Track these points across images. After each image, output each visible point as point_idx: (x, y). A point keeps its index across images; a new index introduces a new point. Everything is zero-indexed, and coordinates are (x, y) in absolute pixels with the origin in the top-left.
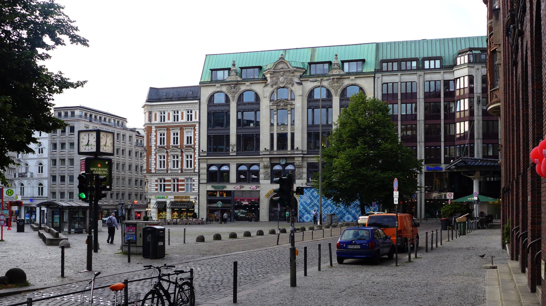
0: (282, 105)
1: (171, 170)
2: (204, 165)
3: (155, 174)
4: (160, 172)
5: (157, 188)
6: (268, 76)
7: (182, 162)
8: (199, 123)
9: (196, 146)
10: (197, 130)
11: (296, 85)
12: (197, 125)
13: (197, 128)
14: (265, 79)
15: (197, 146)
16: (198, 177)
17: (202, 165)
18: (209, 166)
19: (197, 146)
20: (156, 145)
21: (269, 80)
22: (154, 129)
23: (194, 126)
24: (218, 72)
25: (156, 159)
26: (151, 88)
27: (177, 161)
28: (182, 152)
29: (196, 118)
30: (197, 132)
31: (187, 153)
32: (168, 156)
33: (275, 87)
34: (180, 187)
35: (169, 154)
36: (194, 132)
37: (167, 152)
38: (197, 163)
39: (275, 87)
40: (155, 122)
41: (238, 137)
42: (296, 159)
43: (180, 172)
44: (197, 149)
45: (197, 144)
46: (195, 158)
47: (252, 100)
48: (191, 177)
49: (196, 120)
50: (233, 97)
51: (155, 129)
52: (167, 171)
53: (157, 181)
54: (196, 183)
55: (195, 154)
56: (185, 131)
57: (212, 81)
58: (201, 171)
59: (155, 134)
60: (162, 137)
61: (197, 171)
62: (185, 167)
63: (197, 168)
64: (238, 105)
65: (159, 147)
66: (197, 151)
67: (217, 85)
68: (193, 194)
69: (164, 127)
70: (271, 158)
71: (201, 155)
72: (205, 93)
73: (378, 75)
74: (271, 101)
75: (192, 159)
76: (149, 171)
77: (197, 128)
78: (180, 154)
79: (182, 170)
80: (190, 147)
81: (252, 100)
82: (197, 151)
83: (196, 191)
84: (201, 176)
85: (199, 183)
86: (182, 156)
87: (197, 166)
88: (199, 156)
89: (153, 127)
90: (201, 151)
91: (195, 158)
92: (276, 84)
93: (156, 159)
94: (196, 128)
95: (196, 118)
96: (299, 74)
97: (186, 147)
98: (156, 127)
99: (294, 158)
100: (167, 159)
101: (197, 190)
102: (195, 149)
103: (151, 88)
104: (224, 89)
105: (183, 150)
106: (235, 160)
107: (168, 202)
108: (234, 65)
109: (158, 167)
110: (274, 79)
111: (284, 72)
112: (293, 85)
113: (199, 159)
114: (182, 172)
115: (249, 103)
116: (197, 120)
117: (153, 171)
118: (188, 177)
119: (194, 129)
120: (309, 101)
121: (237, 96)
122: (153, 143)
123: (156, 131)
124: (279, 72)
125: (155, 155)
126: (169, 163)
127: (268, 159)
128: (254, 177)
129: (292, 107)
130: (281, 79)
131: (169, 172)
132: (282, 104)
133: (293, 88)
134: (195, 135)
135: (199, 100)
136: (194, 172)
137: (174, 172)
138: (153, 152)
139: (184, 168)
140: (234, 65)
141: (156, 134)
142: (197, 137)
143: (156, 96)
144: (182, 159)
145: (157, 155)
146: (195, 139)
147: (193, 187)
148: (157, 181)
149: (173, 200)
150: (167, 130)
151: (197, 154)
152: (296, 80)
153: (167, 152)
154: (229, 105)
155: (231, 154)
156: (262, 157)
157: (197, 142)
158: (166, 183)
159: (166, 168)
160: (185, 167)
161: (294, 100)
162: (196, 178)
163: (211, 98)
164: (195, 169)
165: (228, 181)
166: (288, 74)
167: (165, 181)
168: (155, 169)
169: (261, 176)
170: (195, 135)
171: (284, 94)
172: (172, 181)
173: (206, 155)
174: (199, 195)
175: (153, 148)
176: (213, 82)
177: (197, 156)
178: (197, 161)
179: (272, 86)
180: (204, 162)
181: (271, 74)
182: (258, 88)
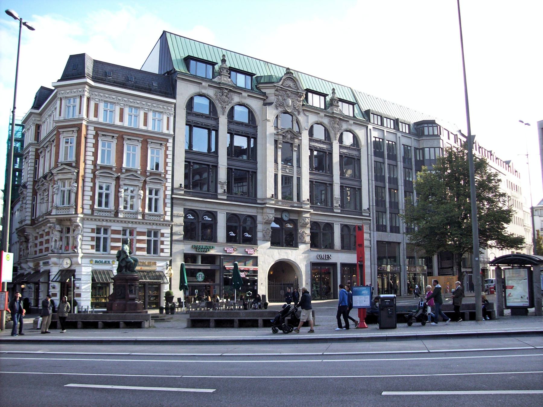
10: (170, 149)
12: (171, 141)
13: (170, 145)
15: (169, 176)
20: (94, 163)
23: (167, 141)
24: (198, 63)
30: (169, 153)
32: (118, 186)
33: (280, 109)
35: (121, 183)
41: (229, 170)
43: (140, 217)
45: (170, 172)
47: (245, 119)
51: (94, 133)
53: (93, 231)
60: (69, 145)
63: (169, 213)
65: (102, 167)
66: (169, 185)
67: (204, 84)
68: (163, 259)
72: (185, 91)
77: (170, 145)
81: (245, 119)
85: (171, 241)
86: (144, 189)
87: (168, 209)
88: (173, 193)
90: (176, 185)
95: (168, 129)
101: (169, 251)
106: (225, 207)
108: (224, 61)
113: (172, 199)
123: (96, 137)
128: (247, 235)
131: (121, 215)
132: (289, 136)
140: (224, 61)
141: (97, 141)
142: (169, 160)
146: (166, 164)
151: (169, 188)
154: (217, 119)
157: (169, 168)
165: (213, 238)
169: (259, 235)
170: (166, 156)
177: (169, 193)
179: (277, 108)
181: (277, 90)
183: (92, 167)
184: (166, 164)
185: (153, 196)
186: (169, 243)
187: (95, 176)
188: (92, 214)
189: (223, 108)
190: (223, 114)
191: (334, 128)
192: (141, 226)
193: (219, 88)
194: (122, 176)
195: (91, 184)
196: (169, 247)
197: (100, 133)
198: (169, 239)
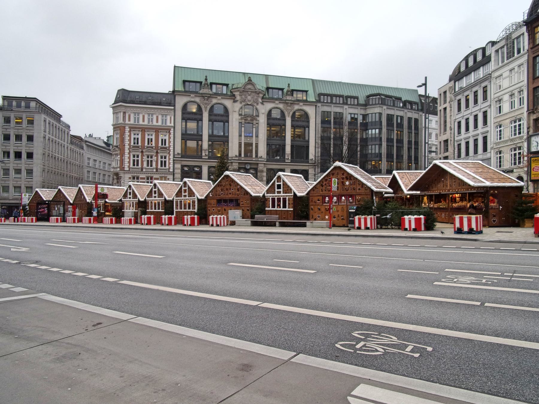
0: (249, 120)
1: (146, 169)
2: (178, 166)
3: (129, 172)
4: (134, 170)
6: (237, 94)
7: (157, 162)
8: (174, 128)
11: (260, 104)
12: (172, 129)
13: (172, 132)
14: (234, 95)
15: (172, 148)
17: (176, 166)
18: (183, 166)
19: (172, 148)
20: (129, 145)
21: (238, 98)
22: (127, 129)
23: (170, 130)
26: (123, 90)
27: (151, 161)
28: (157, 153)
29: (171, 123)
30: (172, 136)
31: (161, 154)
32: (142, 156)
33: (243, 104)
35: (144, 154)
36: (169, 135)
37: (142, 152)
38: (172, 164)
39: (243, 104)
40: (129, 123)
42: (259, 165)
43: (155, 170)
44: (172, 151)
45: (172, 146)
46: (169, 159)
48: (166, 175)
49: (170, 125)
50: (206, 108)
51: (129, 130)
52: (142, 169)
53: (130, 178)
55: (170, 155)
56: (160, 134)
58: (176, 171)
59: (129, 134)
61: (171, 170)
62: (159, 167)
63: (172, 168)
64: (210, 115)
65: (133, 147)
66: (172, 153)
67: (192, 95)
69: (139, 128)
70: (239, 163)
72: (180, 101)
73: (319, 105)
74: (240, 115)
76: (122, 169)
78: (155, 154)
79: (157, 169)
80: (166, 148)
82: (172, 153)
86: (157, 156)
87: (171, 166)
88: (174, 157)
90: (176, 153)
91: (169, 159)
92: (244, 101)
95: (171, 123)
96: (261, 95)
97: (161, 148)
98: (130, 128)
99: (258, 164)
100: (142, 158)
102: (170, 150)
104: (198, 100)
106: (207, 163)
108: (206, 80)
109: (131, 166)
110: (243, 96)
111: (251, 92)
112: (258, 104)
113: (174, 160)
114: (157, 171)
115: (219, 115)
116: (172, 125)
118: (163, 175)
119: (169, 132)
120: (268, 119)
121: (209, 107)
122: (127, 143)
123: (130, 131)
124: (248, 92)
125: (129, 153)
127: (237, 164)
129: (257, 122)
130: (249, 98)
131: (144, 170)
132: (249, 119)
133: (258, 107)
134: (170, 138)
135: (174, 106)
136: (169, 172)
137: (148, 170)
138: (127, 151)
140: (206, 80)
142: (172, 140)
143: (126, 98)
144: (157, 159)
146: (170, 142)
148: (130, 178)
152: (260, 100)
153: (142, 152)
156: (232, 163)
157: (172, 144)
159: (140, 166)
160: (159, 167)
161: (258, 116)
163: (185, 107)
166: (253, 94)
168: (129, 167)
170: (170, 138)
171: (248, 111)
175: (127, 147)
176: (186, 93)
177: (171, 157)
178: (171, 161)
179: (241, 103)
180: (179, 163)
181: (240, 92)
182: (228, 103)
183: (128, 147)
184: (170, 142)
185: (163, 160)
187: (130, 151)
188: (129, 171)
189: (206, 108)
191: (287, 110)
194: (144, 150)
195: (128, 156)
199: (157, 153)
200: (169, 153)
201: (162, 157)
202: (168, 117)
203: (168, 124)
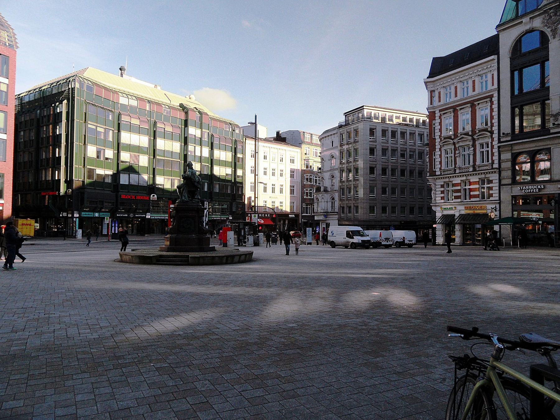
1: (460, 168)
5: (442, 195)
7: (475, 155)
9: (493, 128)
12: (496, 95)
13: (495, 99)
15: (495, 128)
16: (497, 175)
17: (503, 157)
19: (495, 128)
22: (438, 115)
23: (491, 97)
25: (440, 156)
26: (435, 60)
28: (474, 140)
29: (493, 85)
30: (495, 106)
34: (472, 193)
35: (457, 146)
36: (491, 106)
38: (496, 154)
43: (471, 169)
44: (496, 132)
45: (496, 124)
49: (494, 87)
52: (455, 170)
53: (442, 186)
54: (495, 185)
57: (517, 17)
58: (503, 165)
61: (496, 166)
63: (496, 162)
66: (495, 136)
67: (524, 20)
71: (502, 140)
75: (489, 149)
76: (433, 174)
77: (495, 99)
79: (474, 166)
82: (495, 136)
83: (496, 196)
84: (504, 174)
85: (500, 185)
86: (474, 146)
87: (496, 158)
88: (499, 142)
89: (437, 112)
90: (501, 135)
91: (492, 147)
93: (440, 156)
94: (493, 99)
95: (493, 85)
98: (440, 111)
101: (497, 195)
102: (492, 133)
103: (435, 60)
105: (475, 137)
107: (457, 215)
113: (499, 147)
114: (474, 170)
116: (496, 86)
117: (438, 173)
125: (440, 150)
126: (457, 159)
131: (457, 171)
135: (498, 54)
138: (438, 147)
139: (477, 164)
141: (441, 120)
144: (475, 150)
145: (443, 149)
147: (491, 192)
149: (463, 212)
150: (454, 111)
151: (496, 139)
155: (552, 131)
158: (472, 187)
160: (478, 162)
162: (495, 177)
164: (493, 163)
167: (470, 184)
168: (440, 169)
172: (463, 184)
173: (509, 138)
174: (500, 203)
175: (438, 140)
177: (495, 143)
178: (495, 150)
183: (439, 140)
186: (497, 188)
188: (441, 175)
190: (554, 38)
192: (475, 177)
193: (545, 12)
196: (497, 192)
197: (442, 113)
198: (497, 185)
199: (474, 140)
200: (492, 136)
201: (482, 146)
202: (489, 76)
203: (490, 87)
